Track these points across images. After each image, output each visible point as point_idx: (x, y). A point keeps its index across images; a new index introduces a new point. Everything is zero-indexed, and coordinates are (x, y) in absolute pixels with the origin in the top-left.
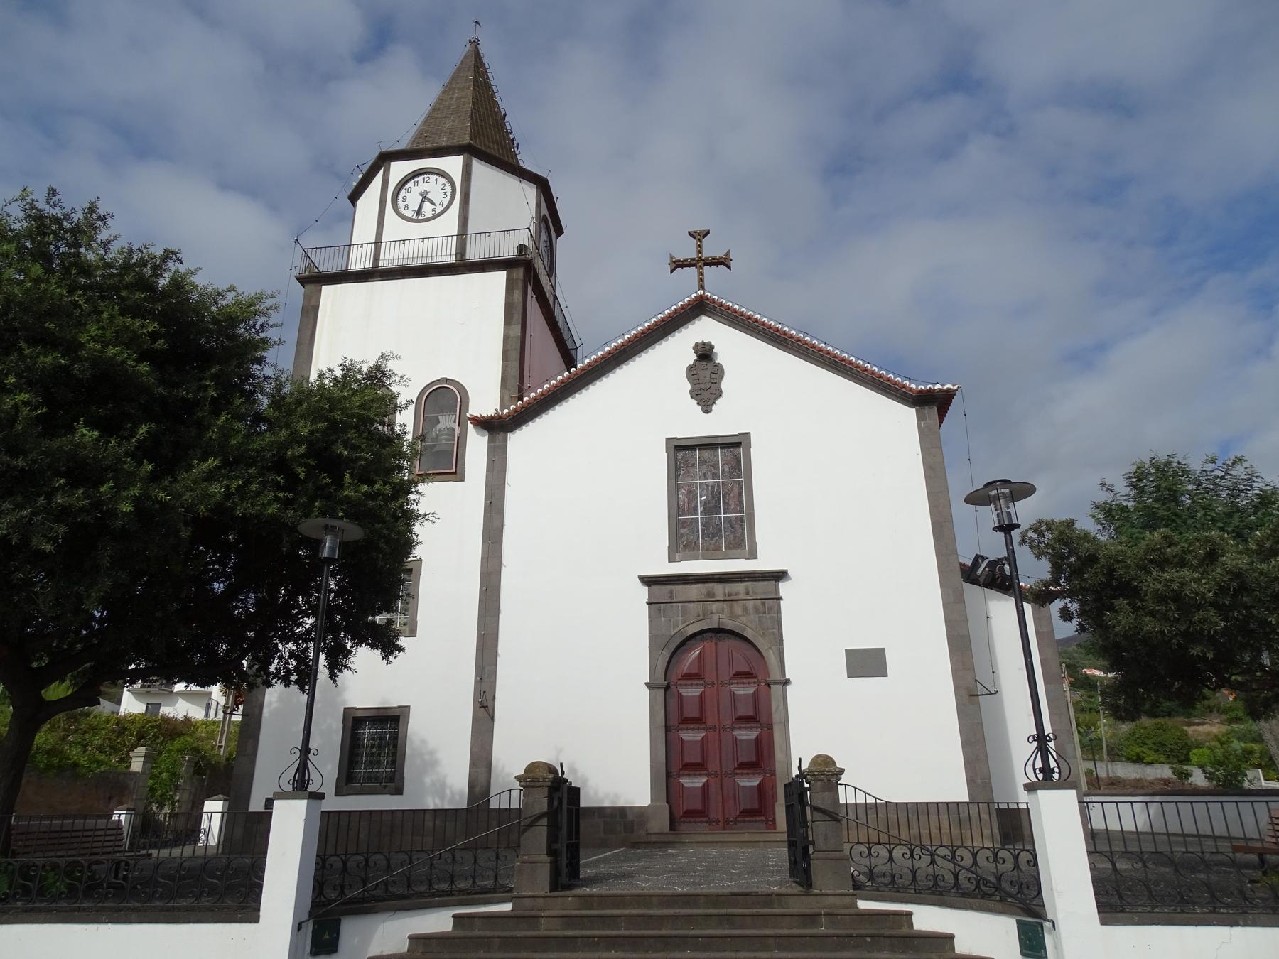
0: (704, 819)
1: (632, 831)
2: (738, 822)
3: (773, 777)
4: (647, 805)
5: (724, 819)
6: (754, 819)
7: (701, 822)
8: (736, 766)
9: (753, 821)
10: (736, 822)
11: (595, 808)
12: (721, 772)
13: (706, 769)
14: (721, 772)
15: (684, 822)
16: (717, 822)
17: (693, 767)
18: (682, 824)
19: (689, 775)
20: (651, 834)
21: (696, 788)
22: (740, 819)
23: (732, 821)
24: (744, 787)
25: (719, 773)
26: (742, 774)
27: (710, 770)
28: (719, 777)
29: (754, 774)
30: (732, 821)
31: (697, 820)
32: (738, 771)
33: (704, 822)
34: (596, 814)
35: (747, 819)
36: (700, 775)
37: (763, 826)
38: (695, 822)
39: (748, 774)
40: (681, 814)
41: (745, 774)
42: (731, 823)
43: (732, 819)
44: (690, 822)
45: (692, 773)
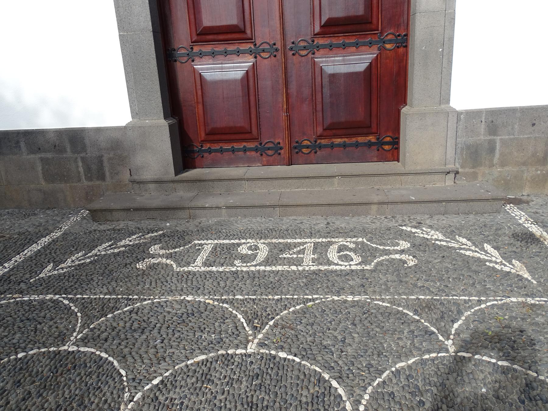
0: (251, 145)
1: (102, 177)
2: (320, 147)
3: (401, 50)
4: (124, 124)
5: (290, 143)
6: (354, 140)
7: (245, 150)
8: (317, 29)
9: (351, 145)
10: (315, 147)
11: (18, 133)
12: (285, 46)
13: (249, 40)
14: (285, 46)
15: (210, 151)
16: (277, 148)
17: (221, 37)
18: (206, 155)
19: (213, 54)
20: (140, 183)
21: (234, 81)
22: (324, 142)
23: (307, 147)
24: (333, 77)
25: (279, 46)
26: (331, 47)
27: (258, 43)
28: (279, 55)
29: (357, 45)
30: (307, 147)
31: (236, 146)
32: (321, 41)
33: (251, 150)
34: (22, 144)
35: (338, 141)
36: (238, 53)
37: (373, 152)
38: (233, 150)
39: (344, 46)
40: (203, 135)
41: (338, 47)
42: (304, 150)
43: (306, 143)
44: (221, 151)
45: (220, 48)
